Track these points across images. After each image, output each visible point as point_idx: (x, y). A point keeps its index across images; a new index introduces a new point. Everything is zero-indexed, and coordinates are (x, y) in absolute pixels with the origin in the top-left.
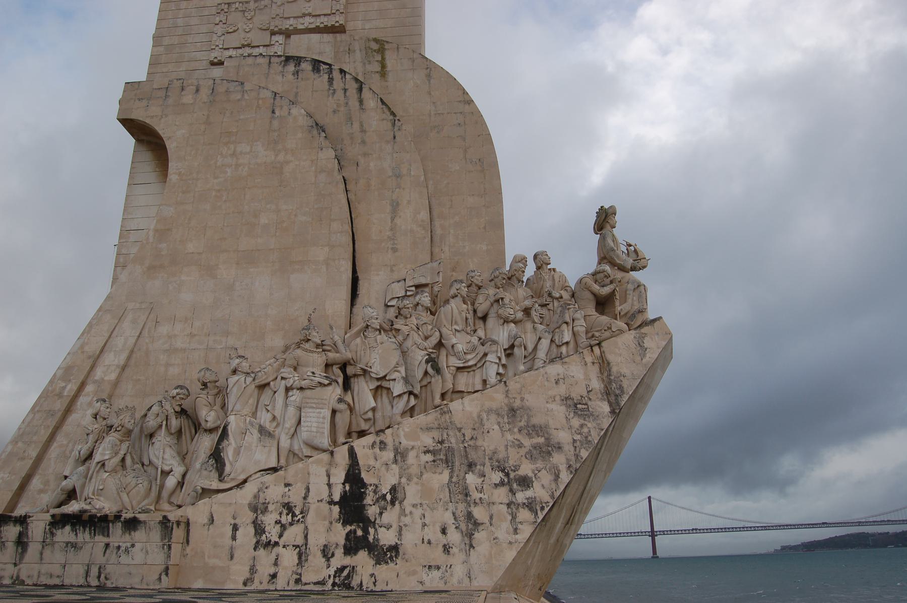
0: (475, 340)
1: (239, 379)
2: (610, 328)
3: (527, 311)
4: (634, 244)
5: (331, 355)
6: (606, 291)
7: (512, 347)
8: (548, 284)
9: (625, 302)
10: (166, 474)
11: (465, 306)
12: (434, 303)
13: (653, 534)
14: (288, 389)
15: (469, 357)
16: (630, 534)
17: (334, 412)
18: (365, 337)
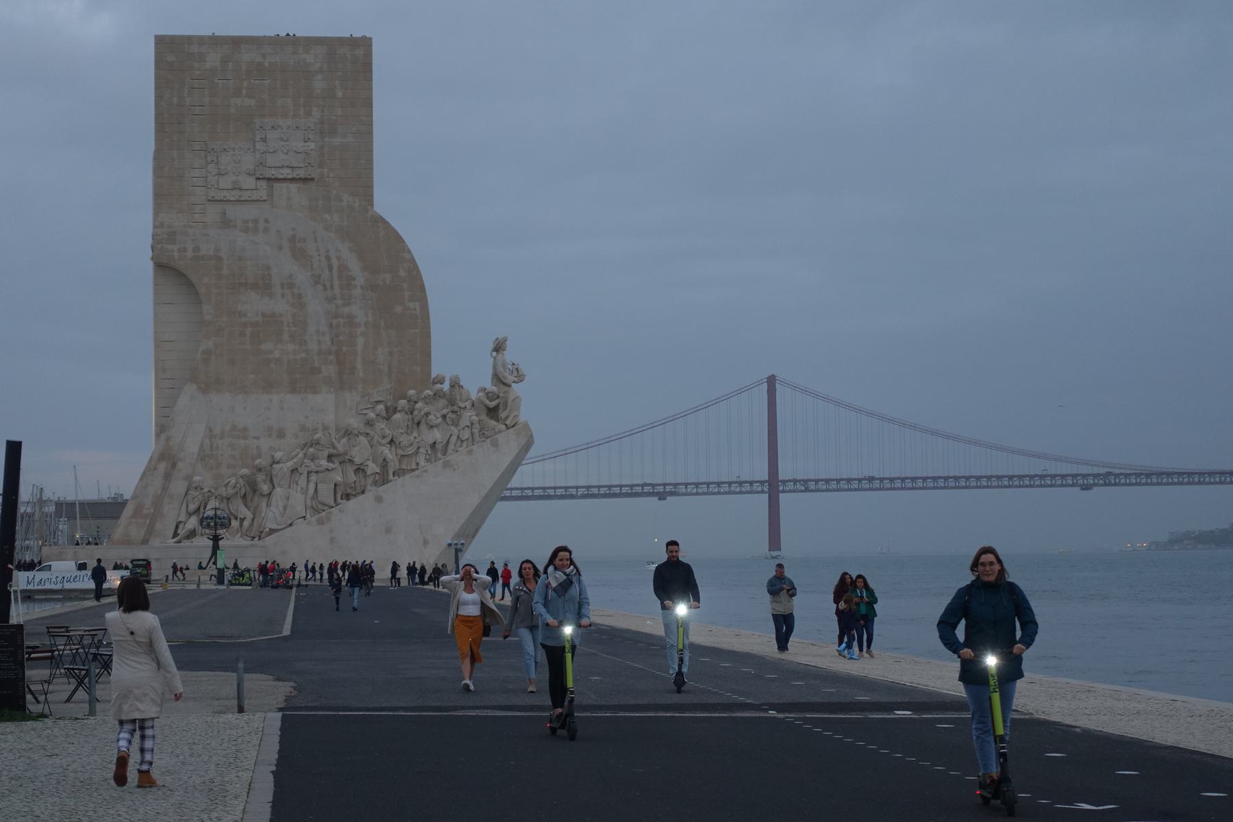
0: (412, 438)
1: (281, 468)
2: (494, 429)
3: (444, 417)
4: (516, 363)
5: (334, 451)
6: (494, 403)
7: (435, 443)
8: (458, 397)
9: (506, 409)
10: (242, 520)
11: (407, 416)
12: (387, 412)
13: (773, 486)
14: (309, 473)
15: (409, 449)
16: (704, 488)
17: (335, 485)
18: (349, 439)
